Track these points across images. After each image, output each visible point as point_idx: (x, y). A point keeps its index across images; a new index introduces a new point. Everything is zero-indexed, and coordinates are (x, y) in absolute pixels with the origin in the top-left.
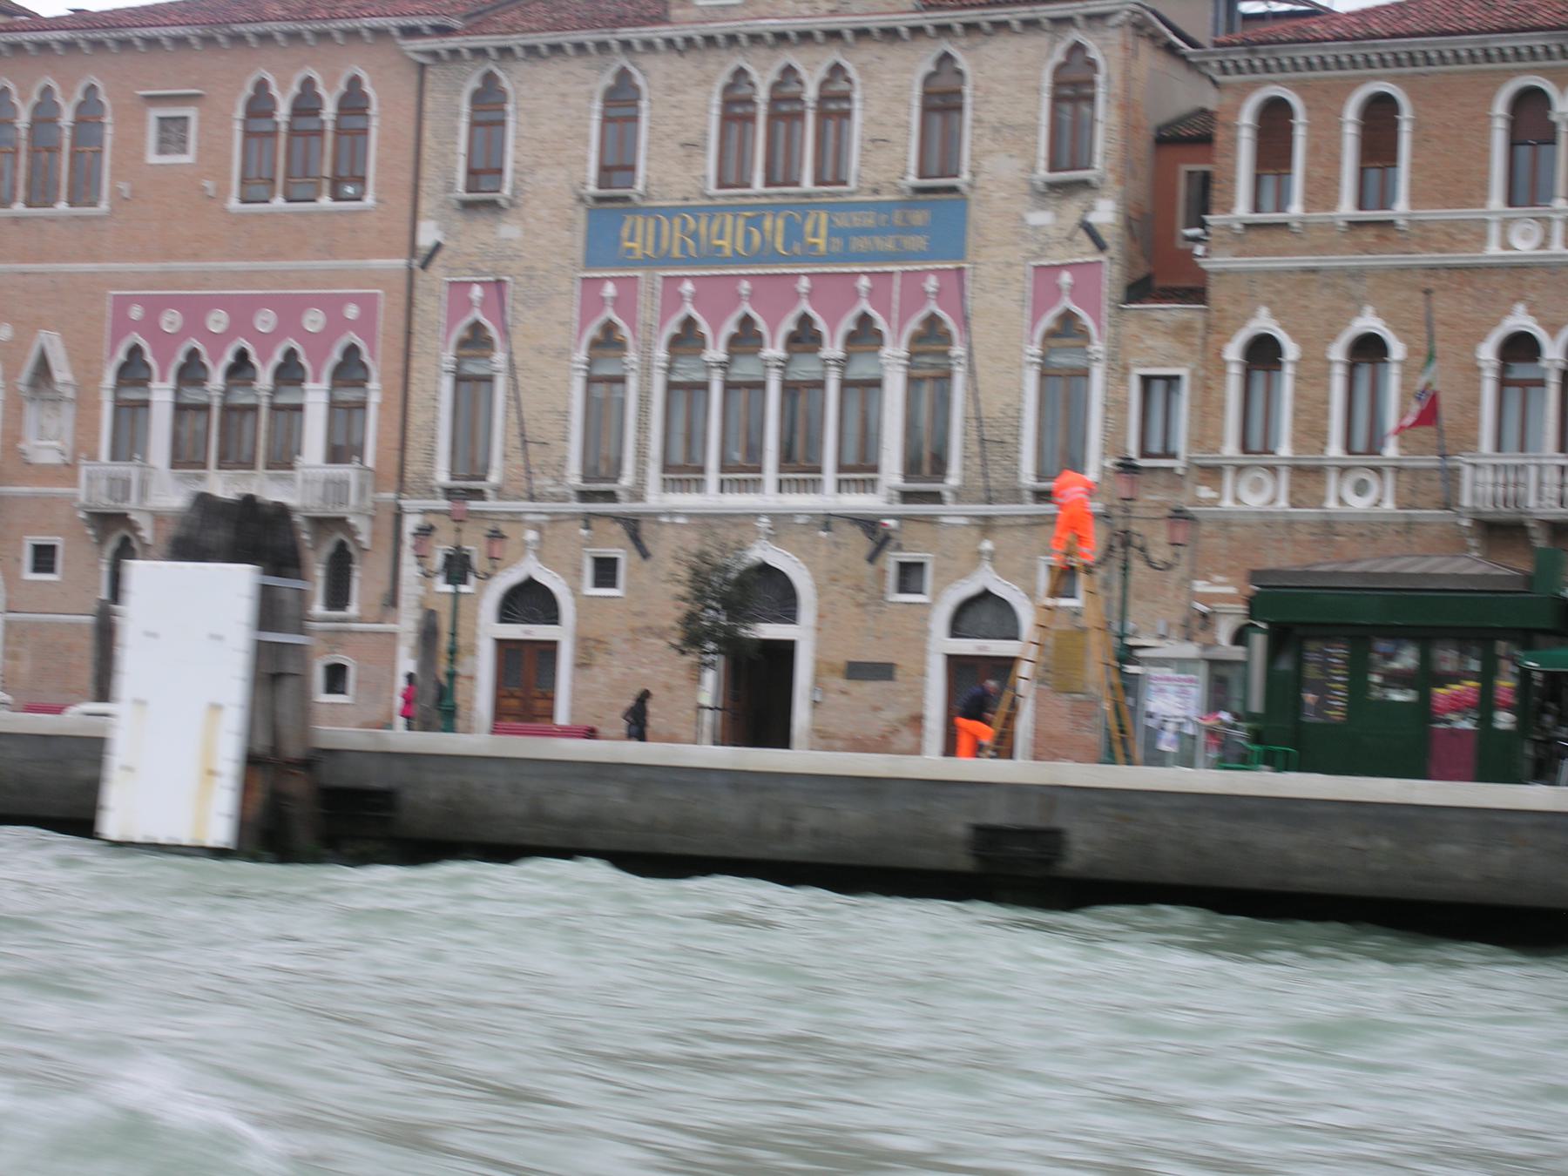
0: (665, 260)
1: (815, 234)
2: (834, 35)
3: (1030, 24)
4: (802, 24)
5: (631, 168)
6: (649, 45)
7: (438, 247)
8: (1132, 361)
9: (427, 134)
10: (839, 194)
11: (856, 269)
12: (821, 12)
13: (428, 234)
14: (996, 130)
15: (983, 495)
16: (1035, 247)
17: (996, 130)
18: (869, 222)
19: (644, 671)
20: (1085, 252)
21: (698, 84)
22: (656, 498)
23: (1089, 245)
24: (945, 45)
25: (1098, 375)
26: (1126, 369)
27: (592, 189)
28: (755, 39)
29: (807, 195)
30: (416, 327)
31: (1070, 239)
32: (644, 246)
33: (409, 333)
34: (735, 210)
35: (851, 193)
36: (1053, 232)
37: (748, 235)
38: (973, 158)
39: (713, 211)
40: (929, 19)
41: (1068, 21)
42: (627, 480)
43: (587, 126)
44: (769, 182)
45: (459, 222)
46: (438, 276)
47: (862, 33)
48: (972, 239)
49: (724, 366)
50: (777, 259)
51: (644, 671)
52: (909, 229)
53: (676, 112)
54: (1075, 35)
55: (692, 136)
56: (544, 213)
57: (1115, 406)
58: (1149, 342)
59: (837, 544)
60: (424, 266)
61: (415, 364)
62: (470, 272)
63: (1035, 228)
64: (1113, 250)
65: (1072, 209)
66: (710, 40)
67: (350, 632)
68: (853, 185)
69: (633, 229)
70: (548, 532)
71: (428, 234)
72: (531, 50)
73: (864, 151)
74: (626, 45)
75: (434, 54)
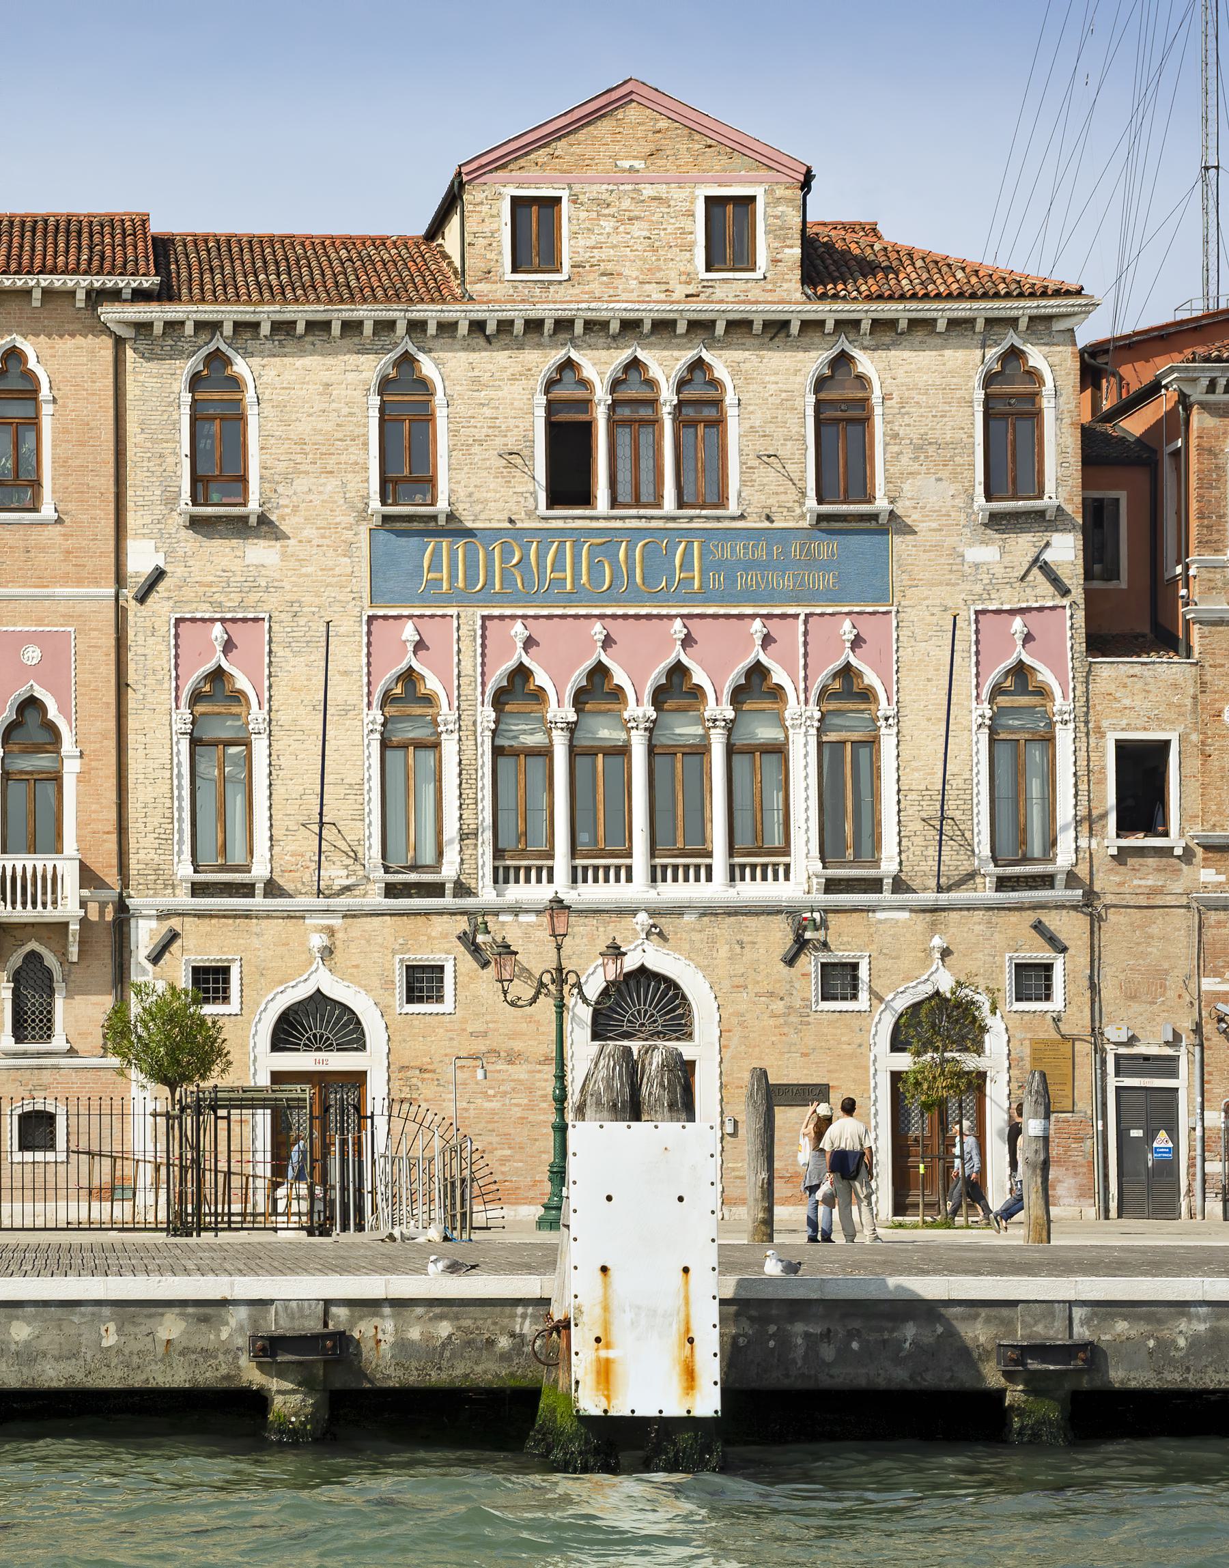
0: (486, 596)
1: (686, 564)
2: (701, 327)
3: (958, 325)
4: (663, 310)
5: (432, 481)
6: (446, 328)
7: (159, 575)
8: (1105, 724)
9: (132, 427)
10: (718, 519)
11: (749, 611)
12: (675, 296)
13: (141, 560)
14: (919, 448)
15: (933, 883)
16: (978, 588)
17: (919, 448)
18: (761, 554)
19: (487, 1105)
20: (1041, 592)
21: (513, 378)
22: (487, 895)
23: (1046, 587)
24: (843, 344)
25: (1064, 738)
26: (1102, 735)
27: (375, 504)
28: (595, 326)
29: (674, 519)
30: (132, 677)
31: (1023, 579)
32: (453, 577)
33: (122, 686)
34: (578, 537)
35: (733, 518)
36: (999, 571)
37: (596, 569)
38: (888, 481)
39: (545, 536)
40: (827, 311)
41: (1013, 322)
42: (449, 871)
43: (366, 425)
44: (614, 503)
45: (189, 541)
46: (161, 607)
47: (740, 326)
48: (898, 578)
49: (572, 728)
50: (636, 598)
51: (487, 1105)
52: (811, 562)
53: (487, 412)
54: (1012, 338)
55: (512, 443)
56: (309, 532)
57: (1086, 775)
58: (1127, 702)
59: (741, 943)
60: (142, 599)
61: (132, 723)
62: (206, 606)
63: (977, 566)
64: (1078, 594)
65: (1023, 545)
66: (534, 326)
67: (57, 1068)
68: (733, 508)
69: (436, 553)
70: (340, 935)
71: (141, 560)
72: (283, 328)
73: (746, 469)
74: (417, 327)
75: (143, 328)
